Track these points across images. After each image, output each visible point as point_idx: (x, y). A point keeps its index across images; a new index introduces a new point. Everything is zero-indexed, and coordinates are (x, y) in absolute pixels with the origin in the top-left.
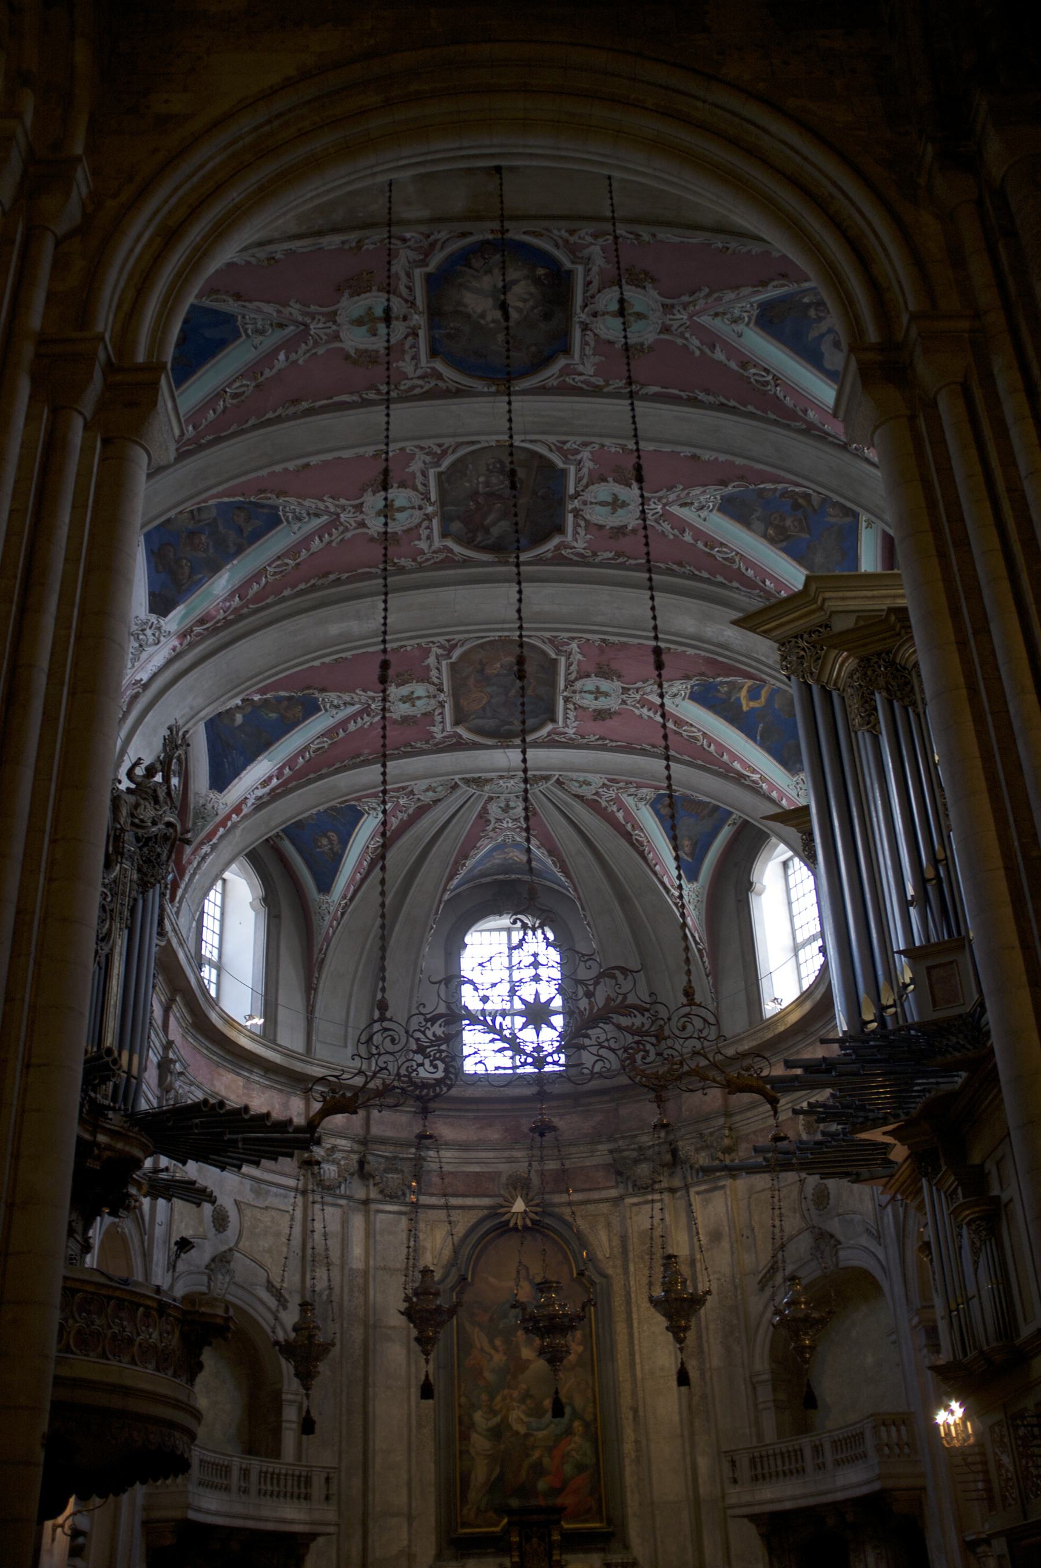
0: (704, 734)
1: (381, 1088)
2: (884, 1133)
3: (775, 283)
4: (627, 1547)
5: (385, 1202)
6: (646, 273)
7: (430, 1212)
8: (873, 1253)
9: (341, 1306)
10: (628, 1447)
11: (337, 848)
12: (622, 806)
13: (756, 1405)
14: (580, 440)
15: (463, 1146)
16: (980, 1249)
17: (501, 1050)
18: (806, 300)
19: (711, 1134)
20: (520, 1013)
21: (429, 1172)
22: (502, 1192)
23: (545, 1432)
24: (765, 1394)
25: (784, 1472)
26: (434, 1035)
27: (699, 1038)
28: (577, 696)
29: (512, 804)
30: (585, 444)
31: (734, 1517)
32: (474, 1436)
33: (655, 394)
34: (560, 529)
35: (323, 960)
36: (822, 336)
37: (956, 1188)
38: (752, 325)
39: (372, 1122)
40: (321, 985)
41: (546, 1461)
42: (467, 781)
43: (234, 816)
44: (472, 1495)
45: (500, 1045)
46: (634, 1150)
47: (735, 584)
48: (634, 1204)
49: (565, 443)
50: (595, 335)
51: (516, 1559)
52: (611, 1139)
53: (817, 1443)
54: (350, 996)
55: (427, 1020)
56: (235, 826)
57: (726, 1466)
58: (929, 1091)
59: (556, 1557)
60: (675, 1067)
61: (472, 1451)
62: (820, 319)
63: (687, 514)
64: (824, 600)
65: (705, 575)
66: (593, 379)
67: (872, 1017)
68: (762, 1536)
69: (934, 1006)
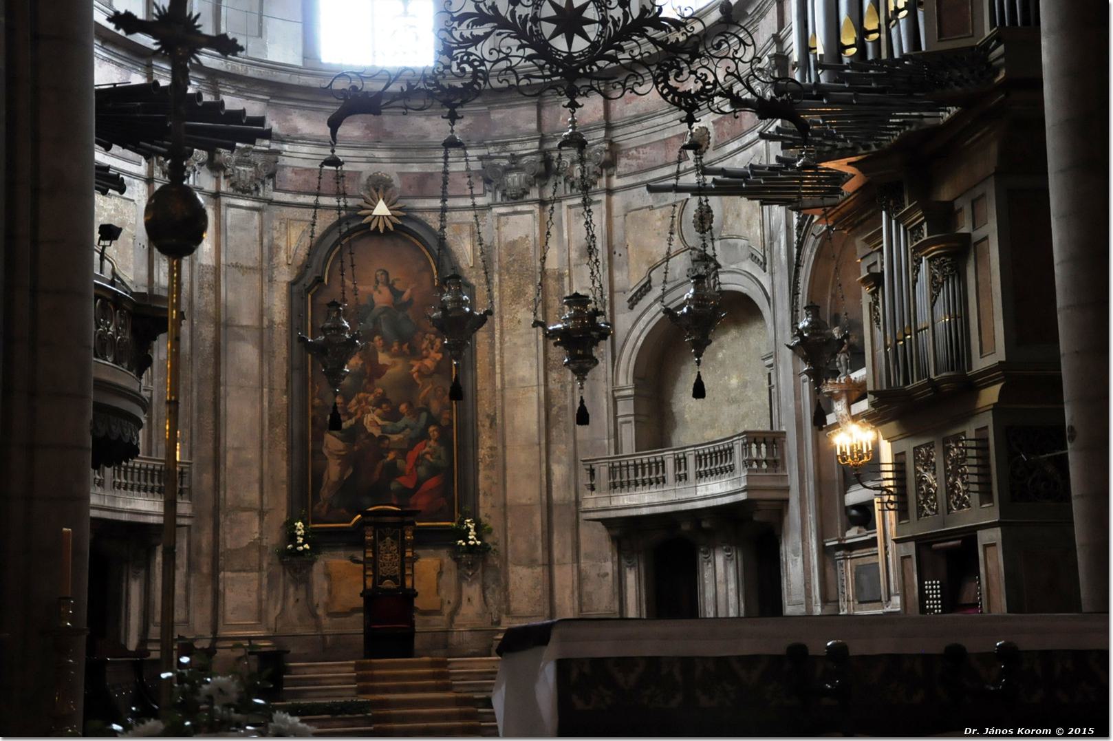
1: (405, 89)
2: (849, 164)
5: (238, 197)
7: (285, 210)
8: (756, 279)
9: (191, 302)
10: (483, 452)
13: (616, 418)
16: (943, 284)
17: (530, 58)
20: (549, 20)
21: (283, 167)
22: (362, 193)
23: (400, 436)
25: (643, 481)
26: (462, 36)
27: (734, 59)
37: (922, 223)
41: (400, 462)
44: (325, 493)
45: (529, 51)
46: (505, 157)
51: (370, 555)
52: (482, 145)
53: (681, 456)
55: (453, 19)
58: (910, 124)
59: (409, 554)
60: (708, 87)
61: (325, 451)
67: (852, 42)
69: (939, 37)
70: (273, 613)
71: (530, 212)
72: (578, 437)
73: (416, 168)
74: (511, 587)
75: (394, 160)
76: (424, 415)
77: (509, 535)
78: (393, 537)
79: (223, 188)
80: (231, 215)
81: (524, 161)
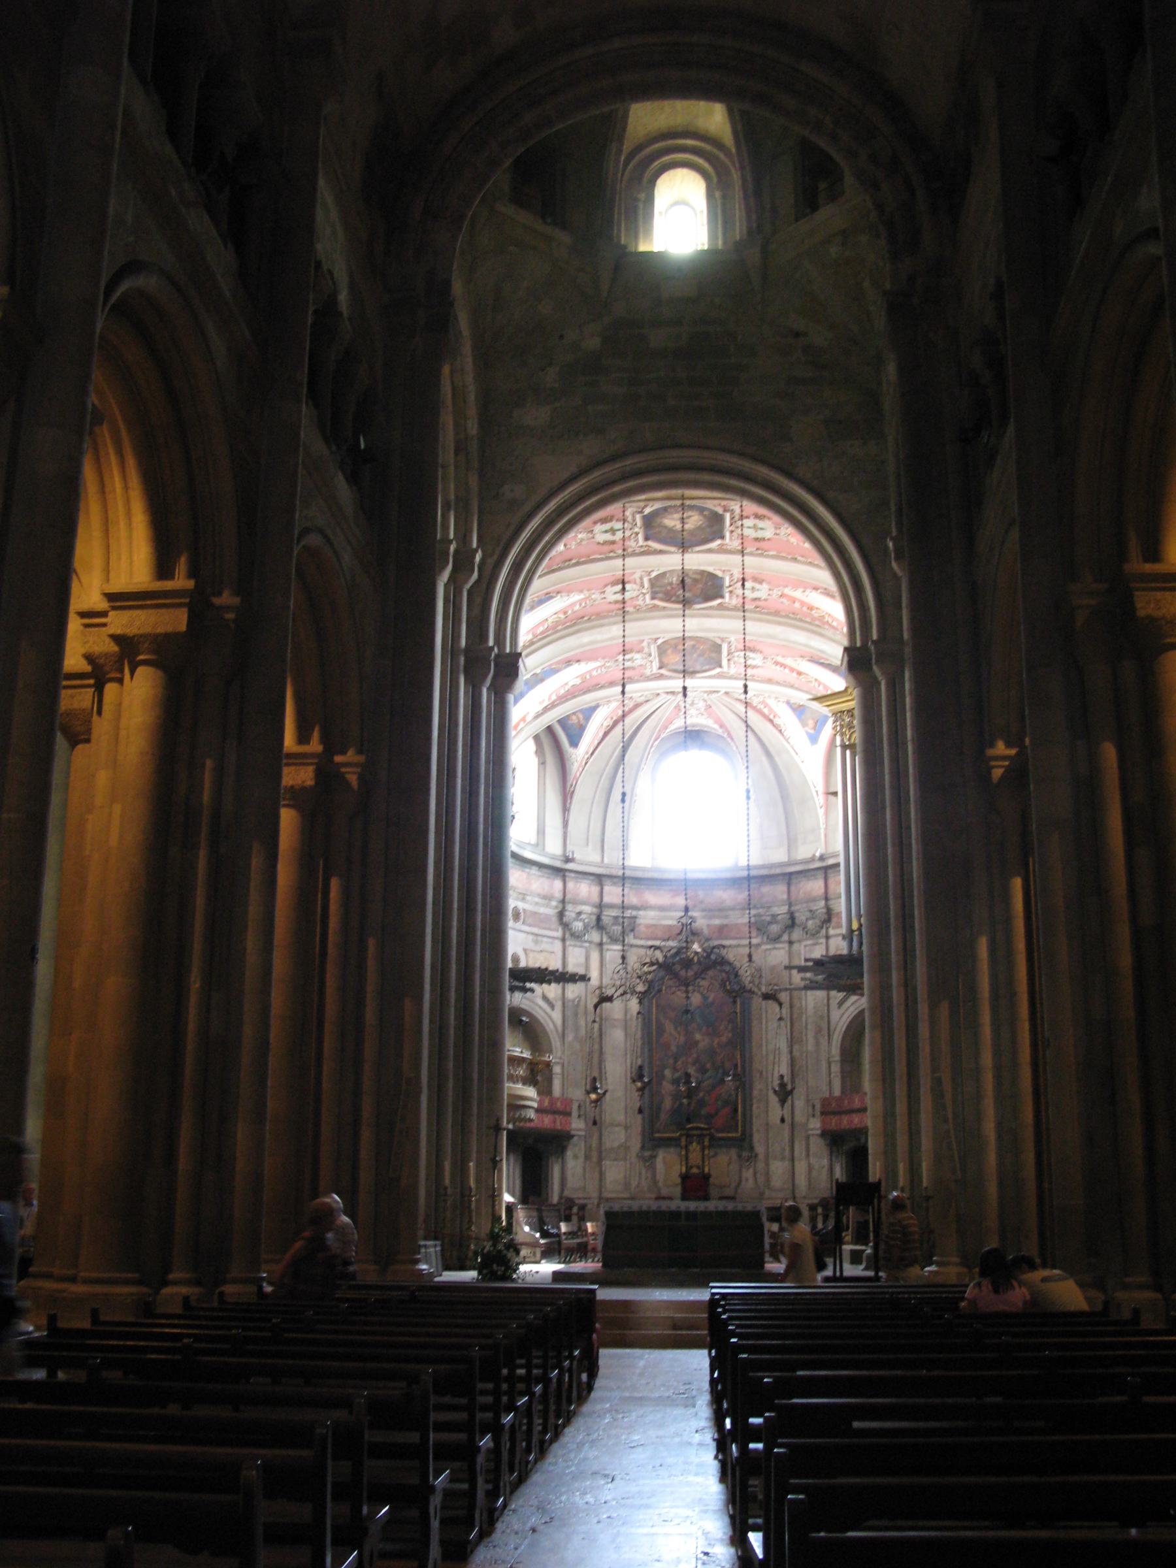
0: (816, 680)
4: (752, 1148)
10: (755, 1093)
11: (582, 722)
12: (766, 705)
15: (662, 908)
19: (817, 910)
21: (639, 925)
24: (836, 1068)
28: (736, 659)
29: (695, 702)
31: (813, 1135)
32: (664, 1083)
34: (722, 597)
35: (573, 792)
39: (604, 894)
40: (572, 807)
41: (707, 1098)
42: (667, 693)
43: (522, 725)
44: (663, 1116)
48: (767, 950)
54: (591, 812)
56: (521, 729)
57: (810, 1109)
59: (706, 1152)
61: (663, 1092)
68: (827, 1145)
70: (634, 1183)
71: (783, 948)
72: (809, 1084)
73: (717, 922)
74: (771, 1173)
75: (704, 917)
76: (720, 1071)
77: (770, 1141)
78: (698, 1143)
79: (604, 940)
80: (608, 955)
81: (779, 918)
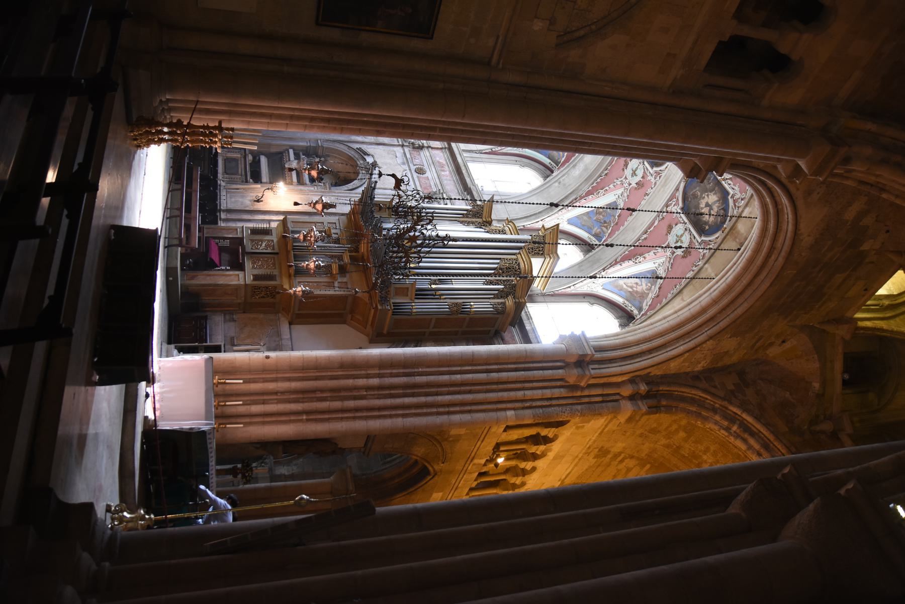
3: (658, 292)
6: (686, 257)
14: (658, 183)
18: (653, 287)
30: (655, 183)
33: (654, 223)
36: (641, 282)
38: (655, 268)
47: (590, 188)
49: (660, 177)
50: (681, 223)
62: (646, 285)
63: (619, 192)
64: (551, 258)
65: (599, 180)
66: (670, 207)
